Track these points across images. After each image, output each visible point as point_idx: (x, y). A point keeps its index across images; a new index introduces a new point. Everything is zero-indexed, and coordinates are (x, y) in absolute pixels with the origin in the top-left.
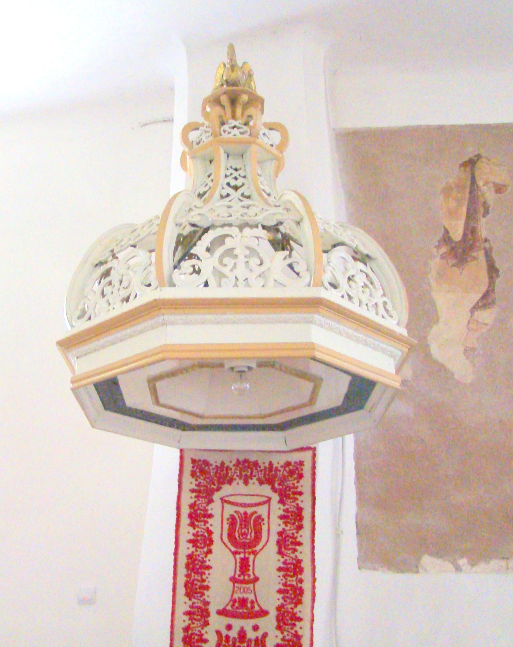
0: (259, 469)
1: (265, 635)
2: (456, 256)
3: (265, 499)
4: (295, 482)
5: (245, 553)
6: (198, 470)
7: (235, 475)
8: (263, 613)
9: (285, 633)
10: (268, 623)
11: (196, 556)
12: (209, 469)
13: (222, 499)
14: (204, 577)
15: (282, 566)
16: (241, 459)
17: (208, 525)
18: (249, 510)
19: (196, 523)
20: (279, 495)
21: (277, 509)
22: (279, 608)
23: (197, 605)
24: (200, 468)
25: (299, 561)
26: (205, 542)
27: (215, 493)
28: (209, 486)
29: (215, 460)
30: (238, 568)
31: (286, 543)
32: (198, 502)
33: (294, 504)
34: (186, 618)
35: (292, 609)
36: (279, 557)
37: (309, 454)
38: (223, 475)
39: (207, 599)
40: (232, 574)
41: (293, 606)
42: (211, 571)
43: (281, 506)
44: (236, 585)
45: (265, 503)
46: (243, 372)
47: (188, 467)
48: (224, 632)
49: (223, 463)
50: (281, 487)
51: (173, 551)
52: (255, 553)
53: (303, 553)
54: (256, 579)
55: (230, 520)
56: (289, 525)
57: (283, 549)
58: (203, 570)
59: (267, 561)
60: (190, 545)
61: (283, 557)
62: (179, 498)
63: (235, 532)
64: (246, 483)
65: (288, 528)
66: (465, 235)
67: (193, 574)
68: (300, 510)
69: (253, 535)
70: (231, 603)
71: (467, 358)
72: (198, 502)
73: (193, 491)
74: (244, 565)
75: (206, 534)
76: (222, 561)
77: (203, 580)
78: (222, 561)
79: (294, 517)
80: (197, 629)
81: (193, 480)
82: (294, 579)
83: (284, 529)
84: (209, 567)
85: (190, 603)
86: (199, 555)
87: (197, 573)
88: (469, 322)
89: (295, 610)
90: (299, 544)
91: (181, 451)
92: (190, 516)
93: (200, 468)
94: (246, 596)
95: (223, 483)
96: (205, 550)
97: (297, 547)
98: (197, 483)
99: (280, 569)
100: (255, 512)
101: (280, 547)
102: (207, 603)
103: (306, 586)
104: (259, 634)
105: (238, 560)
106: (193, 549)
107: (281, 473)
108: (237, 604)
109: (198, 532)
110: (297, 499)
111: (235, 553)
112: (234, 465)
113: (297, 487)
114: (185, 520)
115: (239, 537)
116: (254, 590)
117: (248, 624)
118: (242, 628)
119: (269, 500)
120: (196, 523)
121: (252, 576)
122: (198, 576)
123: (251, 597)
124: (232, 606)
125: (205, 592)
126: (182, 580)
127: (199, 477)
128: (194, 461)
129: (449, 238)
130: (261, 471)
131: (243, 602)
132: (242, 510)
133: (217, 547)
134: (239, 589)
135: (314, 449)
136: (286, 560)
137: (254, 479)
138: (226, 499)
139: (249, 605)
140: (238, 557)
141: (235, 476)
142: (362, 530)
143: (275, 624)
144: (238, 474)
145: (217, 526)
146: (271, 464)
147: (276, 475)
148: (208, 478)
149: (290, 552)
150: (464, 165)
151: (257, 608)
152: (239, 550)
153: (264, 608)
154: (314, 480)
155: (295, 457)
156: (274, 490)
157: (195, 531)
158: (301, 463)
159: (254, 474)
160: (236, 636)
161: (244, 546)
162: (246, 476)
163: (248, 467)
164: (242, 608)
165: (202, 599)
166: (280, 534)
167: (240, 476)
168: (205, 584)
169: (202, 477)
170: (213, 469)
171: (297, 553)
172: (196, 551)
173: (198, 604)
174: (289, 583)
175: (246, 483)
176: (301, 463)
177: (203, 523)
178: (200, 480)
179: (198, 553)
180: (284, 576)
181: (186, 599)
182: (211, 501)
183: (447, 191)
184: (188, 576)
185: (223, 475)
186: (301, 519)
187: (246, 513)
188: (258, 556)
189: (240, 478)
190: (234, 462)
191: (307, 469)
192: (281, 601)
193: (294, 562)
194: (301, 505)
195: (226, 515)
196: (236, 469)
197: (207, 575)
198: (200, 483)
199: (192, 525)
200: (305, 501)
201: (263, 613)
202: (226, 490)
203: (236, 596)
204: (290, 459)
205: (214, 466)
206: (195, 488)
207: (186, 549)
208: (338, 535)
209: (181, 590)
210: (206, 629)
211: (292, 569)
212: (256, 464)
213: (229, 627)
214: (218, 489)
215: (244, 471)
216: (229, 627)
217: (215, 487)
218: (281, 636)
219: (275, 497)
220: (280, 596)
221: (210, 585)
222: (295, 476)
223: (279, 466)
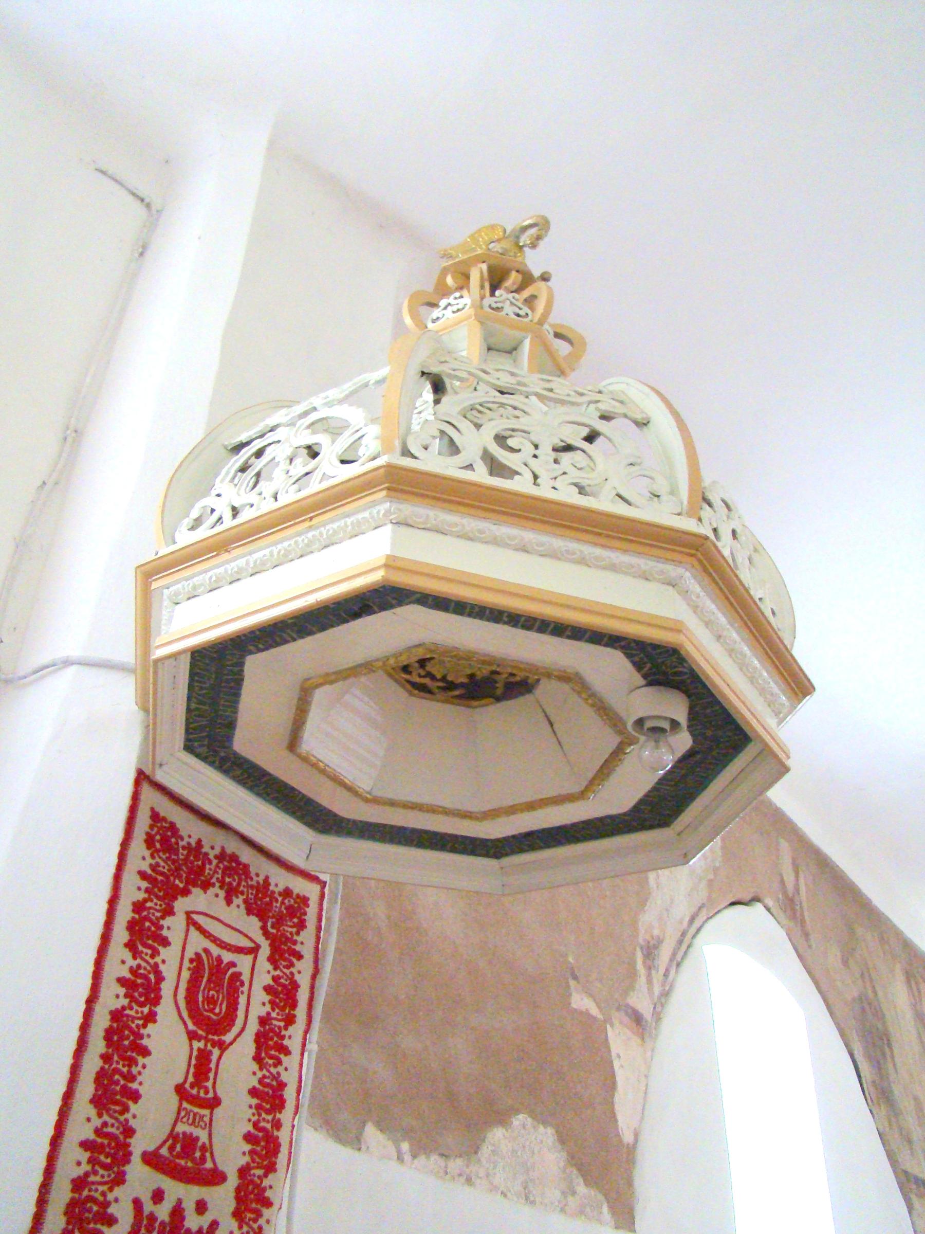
1: (214, 1224)
3: (250, 945)
4: (294, 930)
6: (158, 837)
7: (216, 876)
8: (216, 1178)
10: (222, 1199)
11: (128, 1016)
12: (177, 843)
13: (188, 914)
14: (134, 1070)
16: (229, 851)
18: (227, 957)
20: (270, 945)
22: (243, 1172)
23: (109, 1129)
25: (282, 1085)
26: (146, 995)
27: (180, 898)
28: (172, 878)
29: (191, 829)
30: (192, 1070)
32: (149, 904)
33: (287, 972)
34: (85, 1156)
36: (255, 1067)
39: (132, 1123)
40: (181, 1081)
42: (146, 1060)
44: (185, 1105)
46: (663, 730)
48: (148, 1207)
50: (274, 931)
52: (223, 1047)
54: (215, 1102)
55: (195, 964)
57: (263, 1055)
59: (237, 1069)
63: (198, 992)
65: (274, 1015)
67: (116, 1058)
68: (295, 986)
69: (224, 1006)
70: (170, 1142)
74: (202, 1067)
75: (152, 977)
77: (133, 1078)
80: (101, 1188)
82: (270, 1117)
84: (145, 1052)
85: (97, 1122)
86: (134, 1018)
92: (132, 926)
96: (146, 1010)
98: (153, 862)
99: (253, 1092)
100: (233, 964)
101: (259, 1048)
102: (129, 1132)
104: (204, 1221)
106: (126, 1002)
108: (178, 1148)
109: (139, 966)
111: (192, 1036)
113: (295, 943)
114: (120, 934)
115: (203, 1002)
116: (211, 1124)
117: (190, 1194)
119: (254, 951)
120: (141, 948)
121: (211, 1095)
122: (124, 1066)
123: (203, 1136)
124: (172, 1149)
126: (92, 1064)
127: (158, 851)
128: (155, 816)
130: (252, 887)
131: (189, 1143)
132: (215, 951)
133: (166, 1010)
137: (241, 898)
138: (195, 917)
139: (198, 1154)
140: (197, 1045)
141: (214, 880)
143: (231, 1205)
144: (220, 876)
145: (172, 964)
148: (174, 862)
151: (209, 1165)
152: (200, 1032)
153: (221, 1167)
155: (300, 886)
159: (241, 888)
160: (167, 1219)
162: (230, 884)
164: (185, 1159)
165: (122, 1118)
168: (134, 1086)
169: (161, 854)
170: (184, 848)
179: (132, 1013)
180: (259, 1107)
181: (92, 1112)
182: (169, 912)
187: (219, 959)
189: (221, 888)
190: (217, 851)
192: (247, 1158)
193: (274, 1083)
195: (190, 954)
196: (217, 866)
198: (158, 865)
201: (216, 1178)
202: (198, 900)
203: (181, 1128)
204: (291, 886)
209: (86, 1088)
210: (118, 1192)
213: (158, 1196)
214: (186, 892)
216: (158, 1196)
217: (181, 885)
220: (247, 1147)
221: (142, 1090)
222: (296, 920)
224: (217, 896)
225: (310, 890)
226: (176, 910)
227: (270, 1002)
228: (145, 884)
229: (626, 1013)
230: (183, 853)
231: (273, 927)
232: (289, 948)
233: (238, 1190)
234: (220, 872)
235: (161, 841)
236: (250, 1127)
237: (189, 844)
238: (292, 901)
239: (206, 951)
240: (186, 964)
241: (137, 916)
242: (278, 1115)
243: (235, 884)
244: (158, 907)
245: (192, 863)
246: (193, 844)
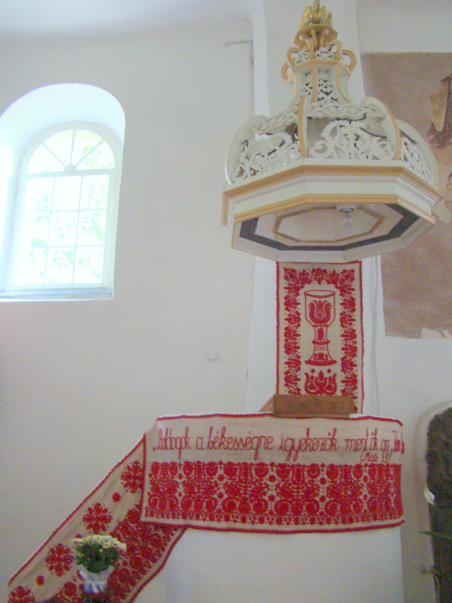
1: (335, 375)
2: (439, 142)
5: (320, 326)
6: (288, 275)
8: (334, 362)
9: (347, 374)
10: (337, 368)
12: (296, 274)
13: (305, 293)
14: (296, 341)
15: (344, 333)
16: (316, 268)
17: (297, 309)
18: (322, 300)
19: (290, 308)
21: (339, 299)
22: (342, 359)
23: (292, 358)
24: (290, 274)
25: (354, 331)
29: (299, 269)
30: (317, 336)
31: (346, 320)
33: (349, 296)
34: (286, 366)
35: (350, 359)
36: (342, 328)
37: (357, 265)
38: (304, 278)
39: (299, 355)
40: (313, 339)
41: (351, 357)
42: (300, 337)
43: (341, 297)
44: (317, 345)
45: (332, 295)
47: (282, 273)
48: (310, 374)
49: (304, 271)
50: (341, 286)
51: (276, 325)
52: (327, 326)
53: (356, 326)
54: (328, 342)
56: (347, 309)
58: (295, 337)
59: (334, 331)
60: (287, 322)
61: (344, 328)
64: (319, 283)
65: (346, 311)
66: (444, 128)
67: (289, 339)
68: (353, 299)
69: (325, 315)
70: (314, 356)
71: (447, 207)
74: (321, 334)
75: (296, 315)
76: (307, 332)
77: (296, 343)
78: (307, 332)
79: (350, 304)
80: (293, 373)
82: (351, 341)
83: (344, 311)
84: (299, 335)
86: (292, 328)
87: (292, 339)
88: (447, 185)
89: (353, 360)
90: (354, 320)
91: (277, 263)
92: (285, 304)
93: (290, 274)
94: (322, 352)
95: (305, 283)
96: (296, 324)
97: (352, 322)
99: (342, 336)
100: (326, 301)
103: (358, 345)
104: (331, 374)
105: (317, 331)
106: (289, 324)
108: (317, 357)
109: (291, 314)
111: (314, 326)
113: (351, 286)
114: (282, 307)
116: (327, 348)
117: (324, 369)
118: (321, 371)
119: (334, 294)
123: (325, 352)
124: (315, 358)
125: (297, 350)
126: (282, 343)
128: (286, 270)
129: (435, 130)
130: (328, 276)
131: (321, 356)
134: (318, 348)
135: (360, 263)
136: (346, 330)
138: (308, 293)
139: (325, 358)
140: (316, 328)
141: (312, 279)
142: (387, 313)
143: (341, 368)
147: (337, 278)
148: (295, 280)
149: (348, 325)
150: (444, 81)
152: (317, 324)
153: (334, 359)
154: (361, 281)
155: (349, 267)
156: (337, 287)
157: (289, 313)
158: (353, 271)
160: (318, 376)
161: (320, 322)
162: (319, 279)
165: (295, 354)
166: (342, 314)
167: (316, 279)
168: (297, 345)
171: (352, 326)
172: (291, 325)
173: (293, 357)
174: (348, 344)
175: (319, 283)
176: (353, 271)
177: (293, 308)
178: (290, 282)
179: (292, 326)
180: (345, 339)
181: (286, 355)
182: (298, 294)
183: (433, 98)
184: (286, 340)
185: (304, 278)
186: (354, 305)
187: (320, 302)
188: (329, 329)
190: (311, 270)
191: (356, 275)
192: (344, 355)
193: (351, 331)
194: (354, 296)
195: (308, 303)
196: (313, 275)
197: (298, 340)
199: (287, 309)
200: (356, 294)
201: (334, 362)
202: (307, 287)
203: (316, 352)
205: (299, 273)
207: (284, 324)
208: (374, 315)
209: (282, 349)
210: (299, 372)
211: (350, 335)
212: (325, 271)
213: (313, 371)
214: (302, 287)
216: (313, 371)
217: (300, 286)
218: (344, 375)
219: (338, 292)
220: (343, 352)
221: (300, 346)
222: (349, 279)
224: (314, 283)
227: (344, 307)
230: (298, 277)
231: (340, 284)
233: (342, 364)
234: (314, 276)
235: (290, 276)
236: (344, 346)
239: (314, 301)
240: (308, 307)
241: (287, 300)
242: (354, 340)
243: (321, 277)
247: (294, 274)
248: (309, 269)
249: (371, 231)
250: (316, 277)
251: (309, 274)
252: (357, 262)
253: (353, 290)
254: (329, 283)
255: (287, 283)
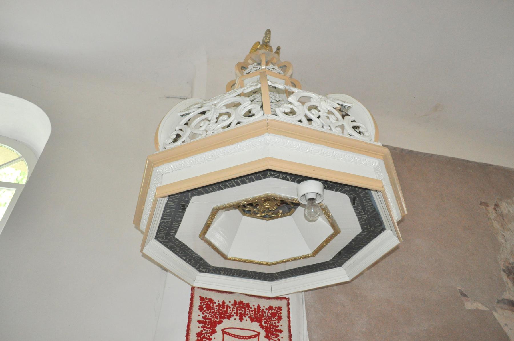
0: (250, 310)
3: (256, 333)
4: (276, 322)
6: (204, 306)
12: (213, 305)
13: (223, 330)
20: (265, 331)
24: (207, 304)
27: (218, 325)
29: (218, 299)
32: (204, 332)
37: (285, 302)
38: (223, 312)
45: (255, 336)
47: (197, 303)
49: (224, 302)
50: (266, 325)
62: (188, 326)
64: (241, 319)
72: (204, 332)
73: (200, 322)
81: (201, 313)
91: (193, 288)
95: (224, 318)
107: (266, 314)
110: (278, 336)
112: (232, 305)
113: (278, 326)
127: (205, 311)
128: (202, 298)
130: (252, 311)
135: (288, 299)
137: (247, 317)
138: (225, 330)
141: (233, 314)
144: (235, 312)
146: (259, 307)
148: (213, 313)
154: (289, 322)
155: (275, 304)
156: (262, 327)
158: (280, 308)
159: (247, 313)
162: (241, 313)
163: (243, 307)
167: (237, 314)
170: (217, 306)
175: (241, 319)
176: (280, 308)
182: (214, 332)
185: (223, 312)
190: (232, 302)
196: (233, 308)
198: (206, 316)
202: (226, 323)
205: (217, 304)
206: (202, 320)
214: (220, 322)
215: (240, 310)
217: (218, 320)
219: (263, 333)
222: (276, 317)
223: (264, 309)
225: (283, 304)
226: (217, 330)
228: (201, 325)
229: (505, 303)
230: (216, 309)
231: (265, 323)
232: (275, 329)
234: (235, 310)
235: (206, 307)
237: (219, 304)
238: (273, 311)
241: (199, 338)
243: (243, 312)
244: (208, 332)
245: (221, 310)
246: (221, 304)
247: (211, 305)
248: (229, 300)
249: (315, 253)
250: (237, 311)
251: (230, 308)
252: (284, 298)
253: (281, 331)
254: (252, 320)
255: (202, 315)
